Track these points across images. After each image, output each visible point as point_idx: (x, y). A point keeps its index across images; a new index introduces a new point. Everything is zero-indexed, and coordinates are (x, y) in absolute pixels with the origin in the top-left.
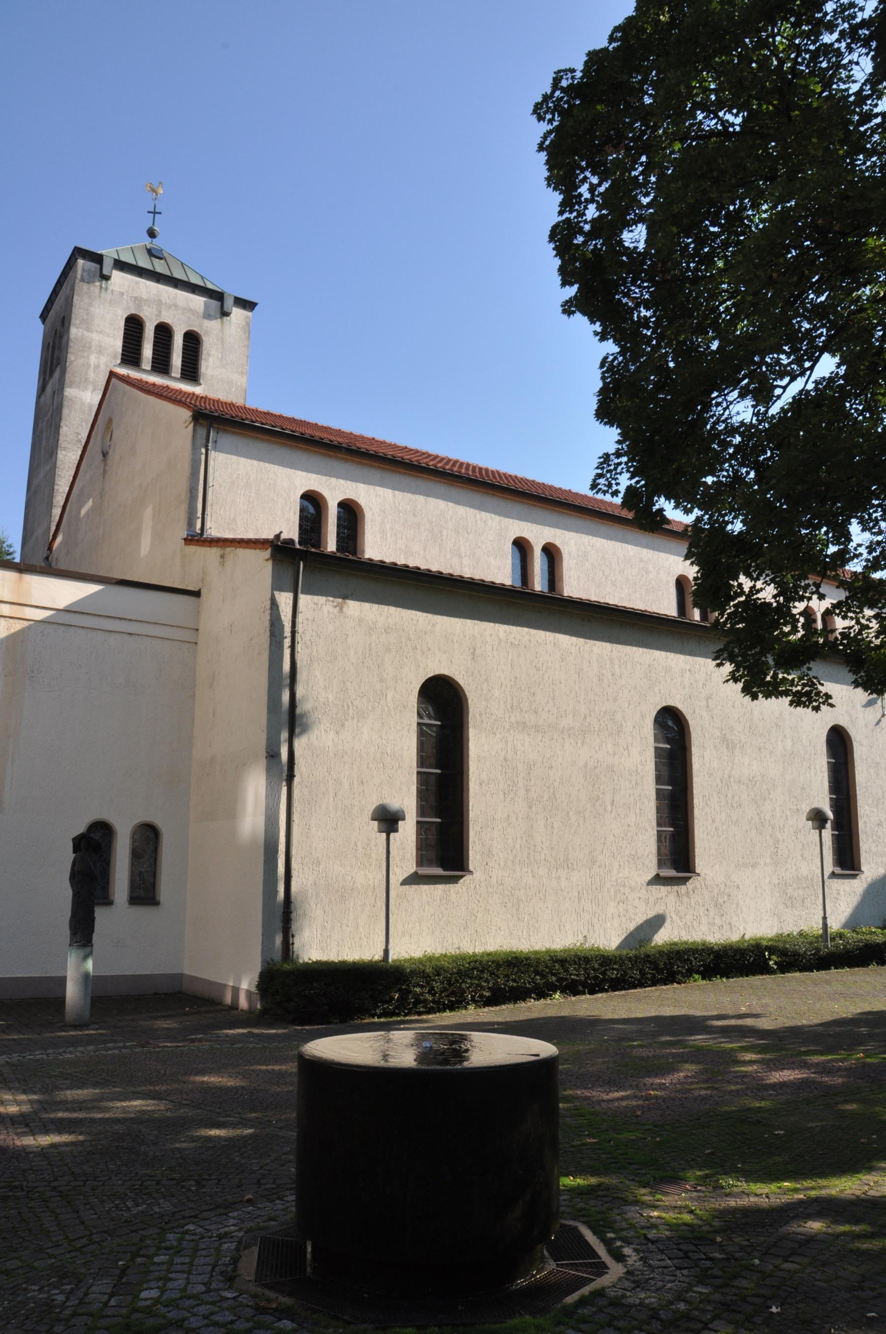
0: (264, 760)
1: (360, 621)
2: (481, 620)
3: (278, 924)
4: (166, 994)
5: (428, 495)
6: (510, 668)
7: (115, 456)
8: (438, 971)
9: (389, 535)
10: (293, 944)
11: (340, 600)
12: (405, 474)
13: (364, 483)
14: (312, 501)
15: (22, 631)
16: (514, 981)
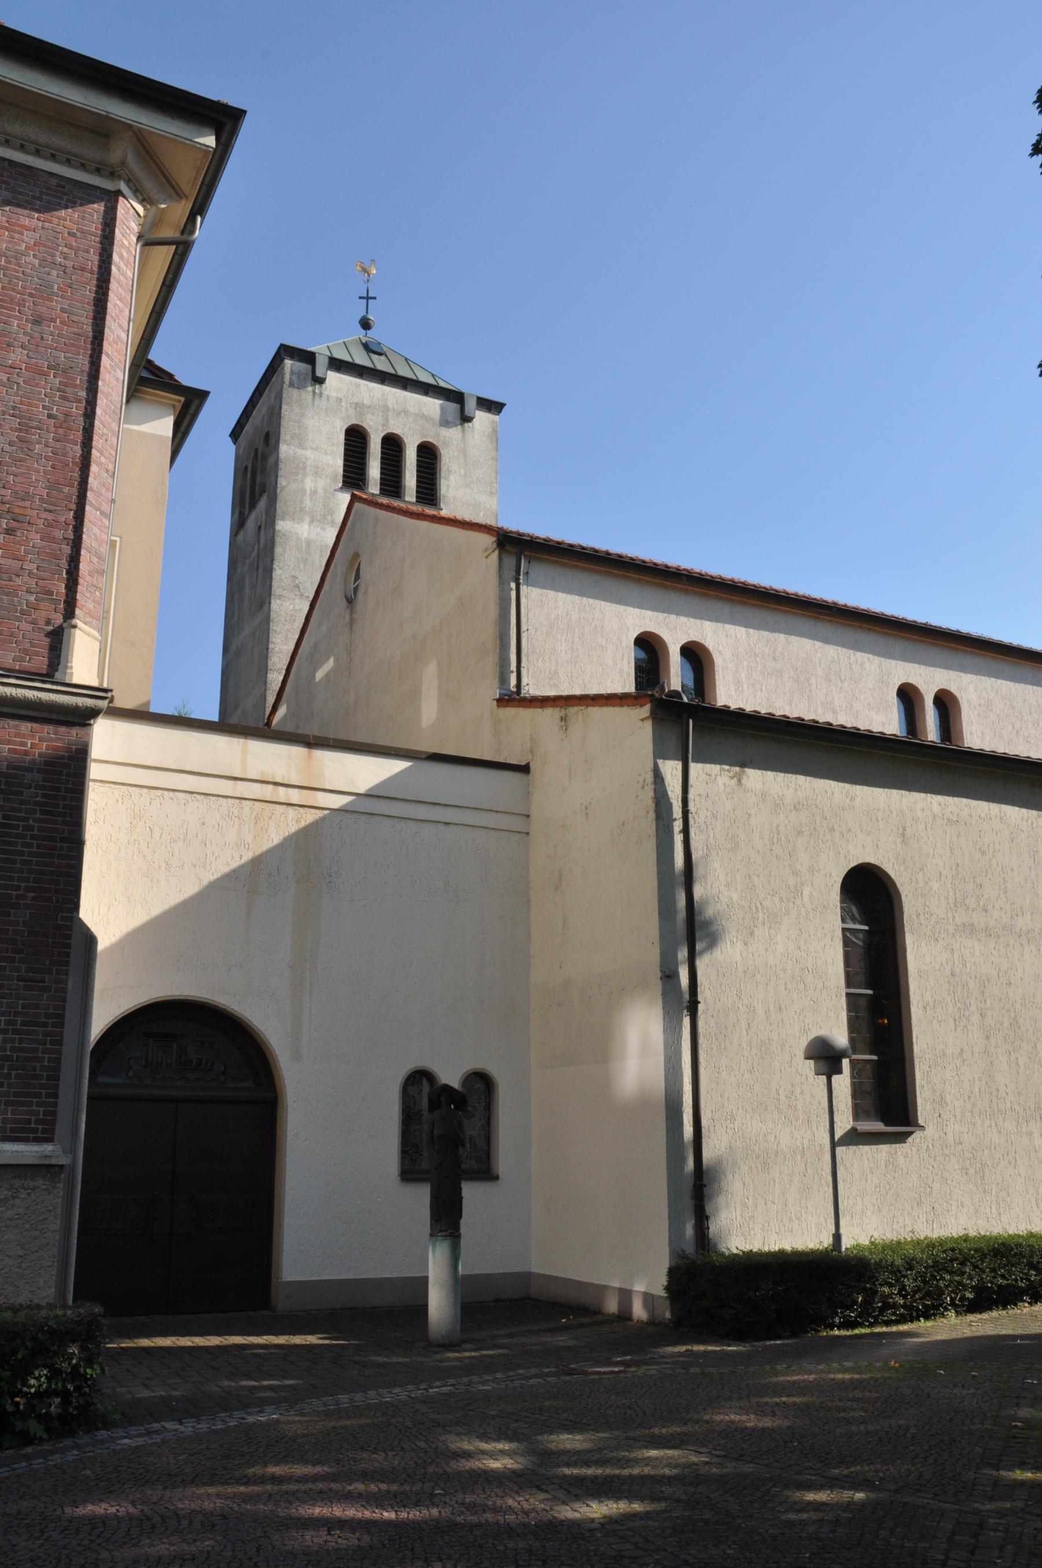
0: (659, 983)
1: (764, 795)
2: (910, 790)
3: (688, 1203)
4: (511, 1300)
5: (790, 633)
6: (948, 851)
7: (368, 600)
8: (910, 1264)
9: (745, 686)
10: (708, 1228)
11: (738, 769)
12: (759, 606)
13: (710, 620)
14: (649, 646)
15: (316, 824)
16: (1003, 1277)
